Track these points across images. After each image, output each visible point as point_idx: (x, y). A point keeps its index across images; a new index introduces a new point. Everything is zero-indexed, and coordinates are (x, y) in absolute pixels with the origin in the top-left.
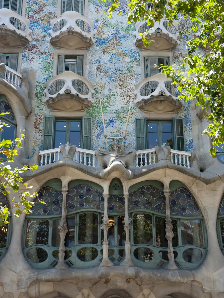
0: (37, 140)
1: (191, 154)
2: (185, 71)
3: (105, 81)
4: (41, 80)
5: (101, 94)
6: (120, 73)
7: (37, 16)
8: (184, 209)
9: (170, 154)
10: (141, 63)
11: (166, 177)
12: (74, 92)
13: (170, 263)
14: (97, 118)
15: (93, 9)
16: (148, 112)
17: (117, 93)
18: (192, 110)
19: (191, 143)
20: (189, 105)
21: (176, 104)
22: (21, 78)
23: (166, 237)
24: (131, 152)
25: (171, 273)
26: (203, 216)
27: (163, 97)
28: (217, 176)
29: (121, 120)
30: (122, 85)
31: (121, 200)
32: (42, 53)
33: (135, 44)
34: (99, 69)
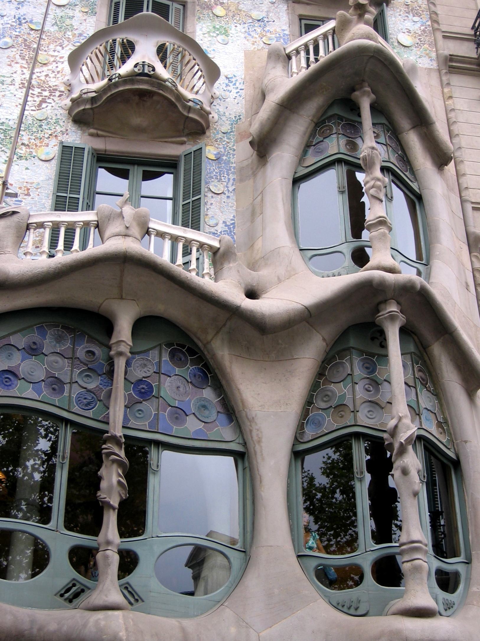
1: (220, 241)
2: (230, 42)
6: (32, 29)
8: (179, 414)
9: (148, 232)
10: (97, 10)
11: (122, 298)
13: (101, 586)
16: (100, 133)
17: (12, 79)
18: (241, 141)
19: (230, 229)
20: (232, 128)
21: (191, 115)
23: (99, 493)
24: (14, 213)
25: (99, 619)
26: (245, 444)
27: (146, 82)
28: (300, 306)
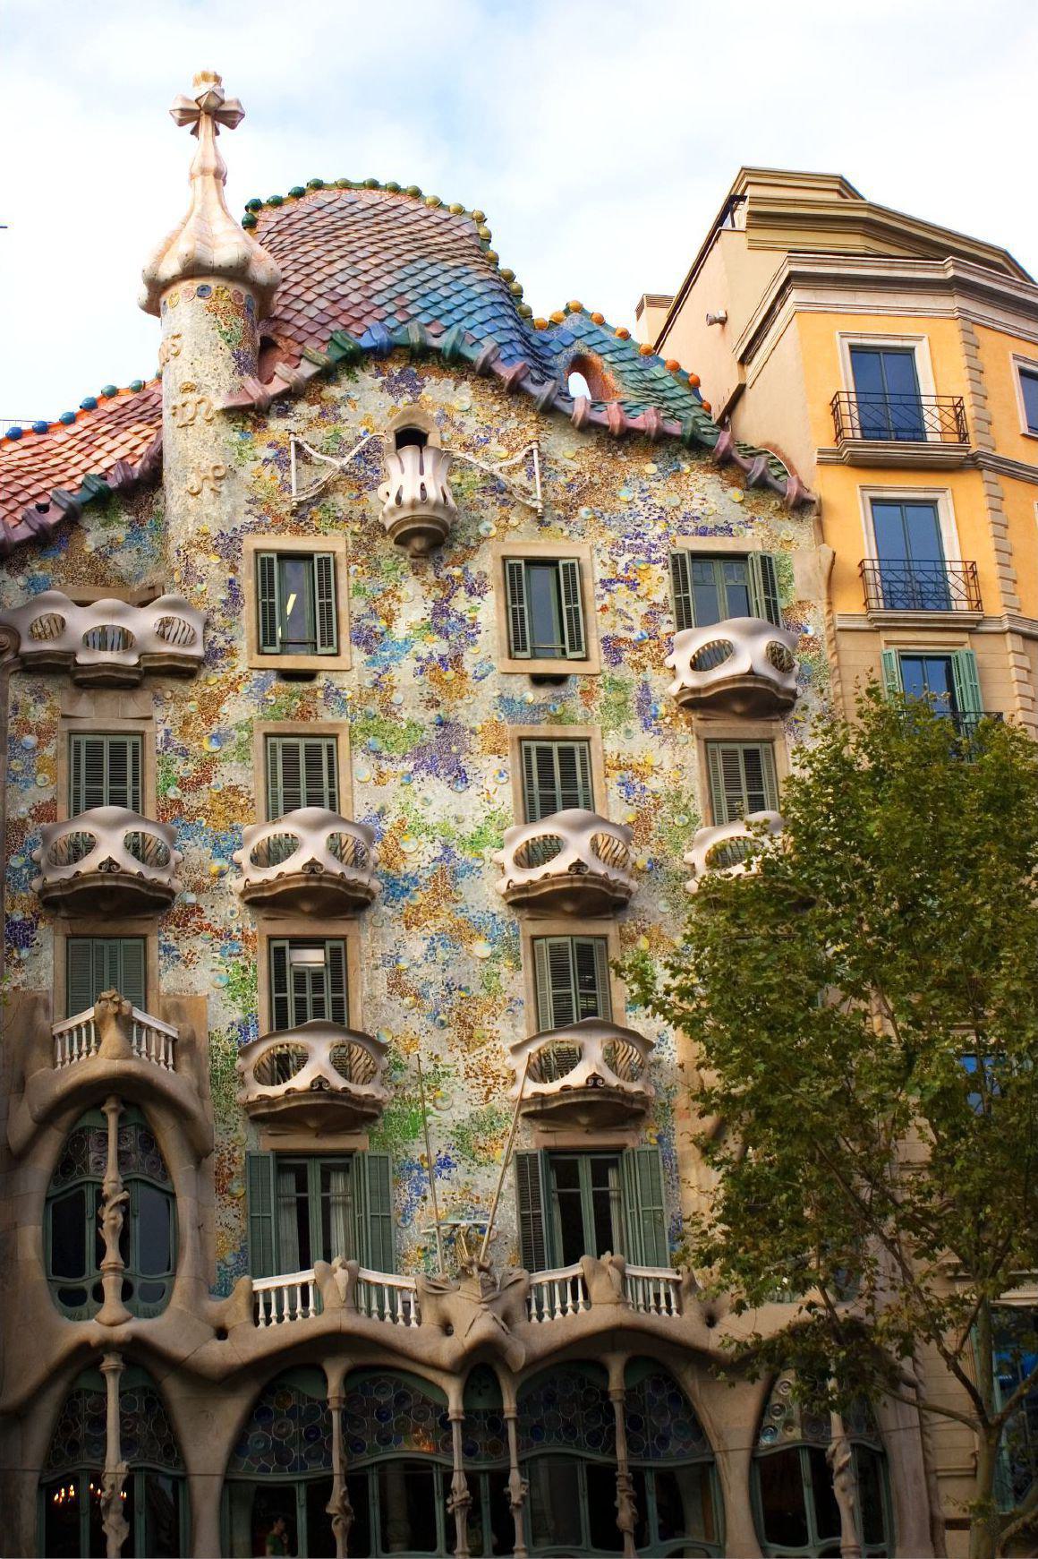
0: (228, 1232)
3: (416, 1027)
4: (224, 1028)
5: (408, 1073)
7: (192, 801)
8: (663, 1441)
12: (338, 1082)
14: (400, 1151)
15: (368, 773)
22: (175, 1040)
29: (473, 1158)
30: (470, 1037)
31: (496, 1422)
32: (218, 935)
33: (504, 896)
34: (397, 985)
